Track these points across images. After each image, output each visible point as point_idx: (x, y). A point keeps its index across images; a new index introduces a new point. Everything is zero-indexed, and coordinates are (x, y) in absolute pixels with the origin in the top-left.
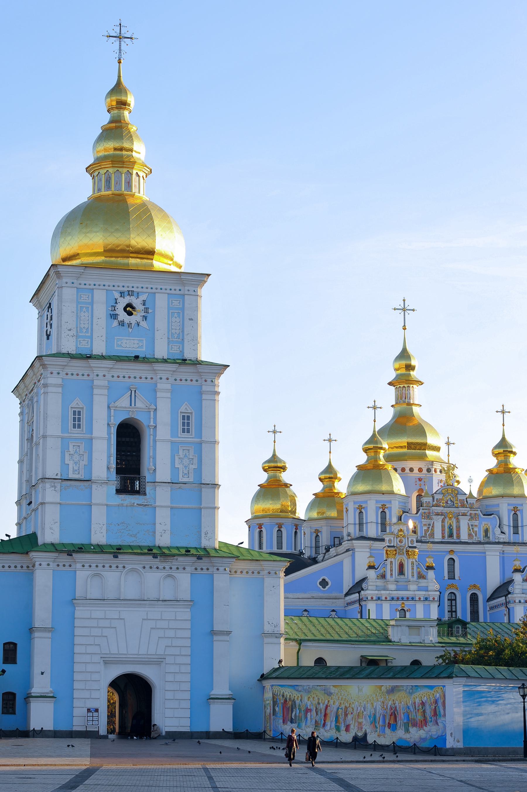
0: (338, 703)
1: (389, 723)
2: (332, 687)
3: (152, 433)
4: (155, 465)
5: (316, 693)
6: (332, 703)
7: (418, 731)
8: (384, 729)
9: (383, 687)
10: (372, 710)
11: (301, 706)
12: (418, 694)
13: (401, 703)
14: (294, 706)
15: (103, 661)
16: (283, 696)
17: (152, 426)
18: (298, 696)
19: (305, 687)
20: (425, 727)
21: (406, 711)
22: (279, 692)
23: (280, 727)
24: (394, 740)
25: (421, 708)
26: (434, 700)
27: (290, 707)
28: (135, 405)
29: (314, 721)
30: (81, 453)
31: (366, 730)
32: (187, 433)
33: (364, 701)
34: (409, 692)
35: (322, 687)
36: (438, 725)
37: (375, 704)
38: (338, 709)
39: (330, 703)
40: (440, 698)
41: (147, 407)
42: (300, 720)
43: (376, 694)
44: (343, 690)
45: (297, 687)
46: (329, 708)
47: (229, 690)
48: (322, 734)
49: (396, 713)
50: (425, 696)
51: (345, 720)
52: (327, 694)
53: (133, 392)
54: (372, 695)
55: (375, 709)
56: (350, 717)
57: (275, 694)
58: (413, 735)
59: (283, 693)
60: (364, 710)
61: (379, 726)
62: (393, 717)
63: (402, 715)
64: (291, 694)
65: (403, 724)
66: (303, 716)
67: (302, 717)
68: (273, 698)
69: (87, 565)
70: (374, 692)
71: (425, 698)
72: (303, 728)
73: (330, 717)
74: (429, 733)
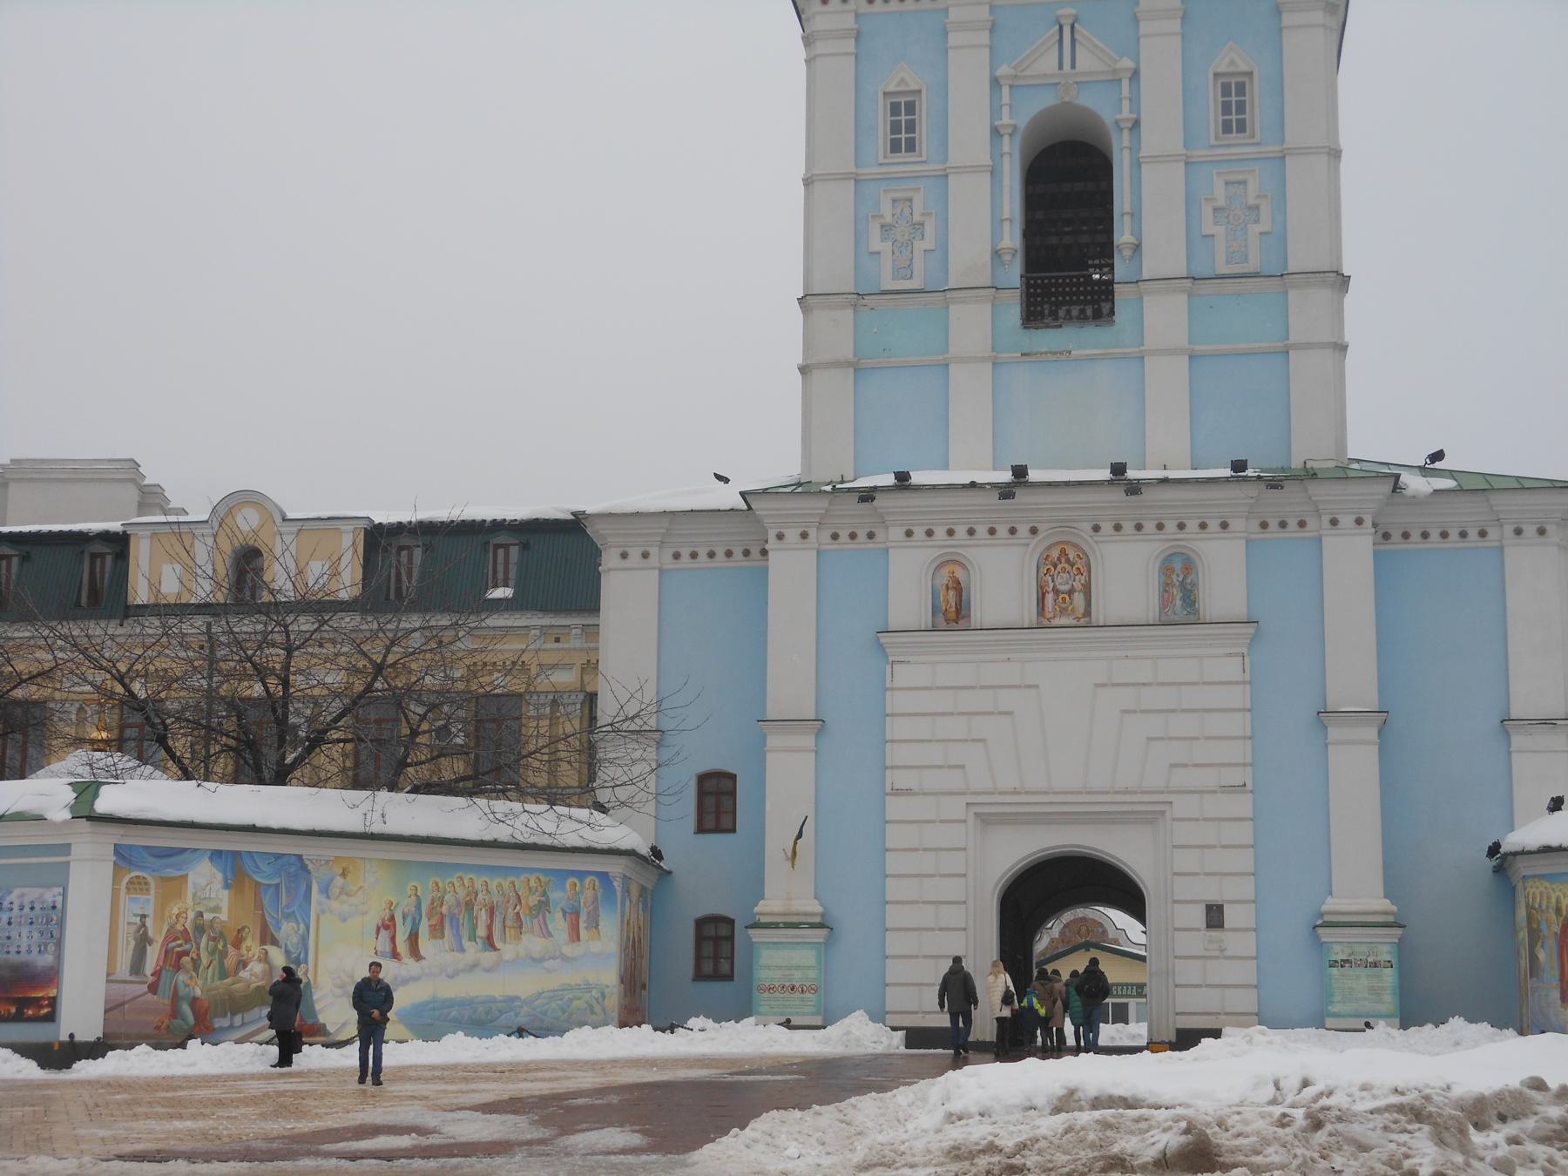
3: (1126, 143)
4: (1136, 231)
15: (976, 814)
16: (1558, 910)
17: (1127, 120)
22: (1545, 899)
28: (1073, 66)
30: (917, 218)
32: (1237, 132)
41: (1109, 66)
47: (1386, 897)
53: (1067, 33)
57: (1533, 908)
59: (1558, 901)
68: (1530, 918)
69: (919, 532)
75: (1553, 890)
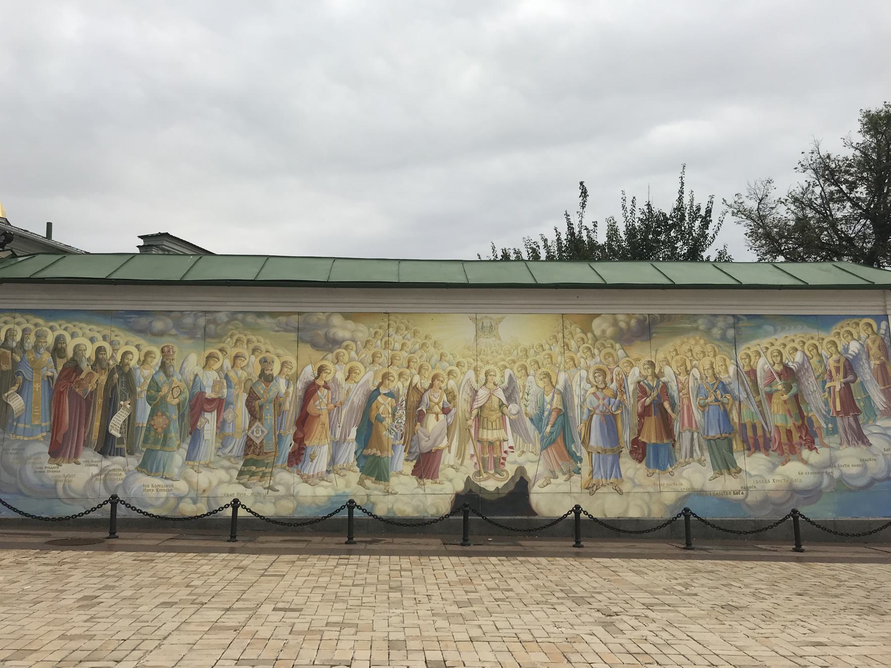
0: (369, 375)
1: (635, 442)
2: (337, 320)
5: (248, 341)
6: (341, 376)
7: (775, 466)
8: (616, 463)
9: (596, 323)
10: (548, 399)
11: (165, 390)
12: (765, 342)
13: (688, 372)
14: (119, 389)
16: (58, 351)
18: (148, 354)
19: (188, 320)
20: (805, 453)
21: (711, 399)
23: (29, 472)
24: (669, 497)
25: (780, 387)
26: (838, 361)
27: (101, 393)
29: (237, 445)
31: (521, 470)
33: (506, 367)
34: (723, 338)
35: (283, 319)
36: (867, 443)
37: (562, 377)
38: (372, 396)
39: (327, 377)
40: (864, 357)
42: (156, 442)
43: (566, 346)
44: (397, 330)
45: (143, 321)
46: (322, 393)
48: (282, 490)
49: (666, 405)
50: (796, 350)
51: (409, 438)
52: (315, 345)
54: (547, 347)
55: (565, 396)
56: (434, 424)
58: (758, 479)
60: (511, 398)
61: (589, 453)
62: (651, 423)
63: (697, 415)
64: (106, 345)
65: (705, 445)
66: (174, 428)
67: (166, 432)
70: (555, 337)
71: (798, 357)
72: (176, 471)
73: (332, 428)
74: (829, 470)
75: (51, 328)
